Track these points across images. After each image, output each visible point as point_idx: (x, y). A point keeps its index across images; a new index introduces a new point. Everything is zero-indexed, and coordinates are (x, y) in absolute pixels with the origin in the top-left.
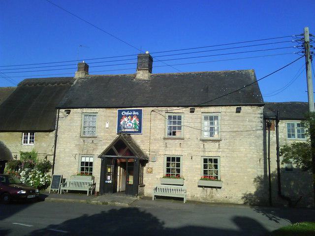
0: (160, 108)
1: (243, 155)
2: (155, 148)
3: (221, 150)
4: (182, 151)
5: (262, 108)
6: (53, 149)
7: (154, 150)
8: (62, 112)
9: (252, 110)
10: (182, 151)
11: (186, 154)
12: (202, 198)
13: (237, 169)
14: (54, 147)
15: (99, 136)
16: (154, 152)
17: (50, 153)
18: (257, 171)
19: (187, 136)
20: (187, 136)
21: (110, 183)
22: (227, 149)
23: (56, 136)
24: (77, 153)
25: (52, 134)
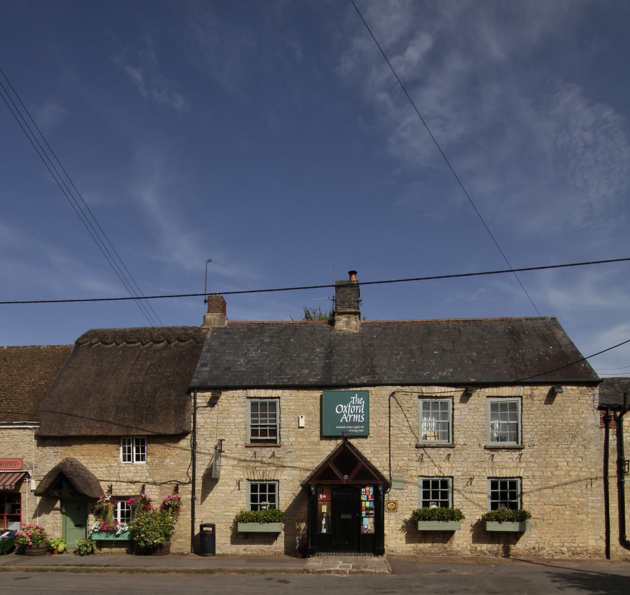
0: (407, 388)
1: (562, 473)
3: (523, 465)
4: (452, 468)
5: (597, 390)
6: (190, 471)
7: (399, 468)
8: (202, 398)
9: (578, 392)
10: (452, 468)
11: (460, 474)
12: (490, 552)
13: (552, 499)
14: (191, 467)
15: (285, 444)
16: (399, 472)
17: (183, 480)
18: (588, 500)
19: (460, 440)
20: (460, 440)
22: (535, 462)
23: (194, 445)
24: (242, 477)
25: (185, 443)
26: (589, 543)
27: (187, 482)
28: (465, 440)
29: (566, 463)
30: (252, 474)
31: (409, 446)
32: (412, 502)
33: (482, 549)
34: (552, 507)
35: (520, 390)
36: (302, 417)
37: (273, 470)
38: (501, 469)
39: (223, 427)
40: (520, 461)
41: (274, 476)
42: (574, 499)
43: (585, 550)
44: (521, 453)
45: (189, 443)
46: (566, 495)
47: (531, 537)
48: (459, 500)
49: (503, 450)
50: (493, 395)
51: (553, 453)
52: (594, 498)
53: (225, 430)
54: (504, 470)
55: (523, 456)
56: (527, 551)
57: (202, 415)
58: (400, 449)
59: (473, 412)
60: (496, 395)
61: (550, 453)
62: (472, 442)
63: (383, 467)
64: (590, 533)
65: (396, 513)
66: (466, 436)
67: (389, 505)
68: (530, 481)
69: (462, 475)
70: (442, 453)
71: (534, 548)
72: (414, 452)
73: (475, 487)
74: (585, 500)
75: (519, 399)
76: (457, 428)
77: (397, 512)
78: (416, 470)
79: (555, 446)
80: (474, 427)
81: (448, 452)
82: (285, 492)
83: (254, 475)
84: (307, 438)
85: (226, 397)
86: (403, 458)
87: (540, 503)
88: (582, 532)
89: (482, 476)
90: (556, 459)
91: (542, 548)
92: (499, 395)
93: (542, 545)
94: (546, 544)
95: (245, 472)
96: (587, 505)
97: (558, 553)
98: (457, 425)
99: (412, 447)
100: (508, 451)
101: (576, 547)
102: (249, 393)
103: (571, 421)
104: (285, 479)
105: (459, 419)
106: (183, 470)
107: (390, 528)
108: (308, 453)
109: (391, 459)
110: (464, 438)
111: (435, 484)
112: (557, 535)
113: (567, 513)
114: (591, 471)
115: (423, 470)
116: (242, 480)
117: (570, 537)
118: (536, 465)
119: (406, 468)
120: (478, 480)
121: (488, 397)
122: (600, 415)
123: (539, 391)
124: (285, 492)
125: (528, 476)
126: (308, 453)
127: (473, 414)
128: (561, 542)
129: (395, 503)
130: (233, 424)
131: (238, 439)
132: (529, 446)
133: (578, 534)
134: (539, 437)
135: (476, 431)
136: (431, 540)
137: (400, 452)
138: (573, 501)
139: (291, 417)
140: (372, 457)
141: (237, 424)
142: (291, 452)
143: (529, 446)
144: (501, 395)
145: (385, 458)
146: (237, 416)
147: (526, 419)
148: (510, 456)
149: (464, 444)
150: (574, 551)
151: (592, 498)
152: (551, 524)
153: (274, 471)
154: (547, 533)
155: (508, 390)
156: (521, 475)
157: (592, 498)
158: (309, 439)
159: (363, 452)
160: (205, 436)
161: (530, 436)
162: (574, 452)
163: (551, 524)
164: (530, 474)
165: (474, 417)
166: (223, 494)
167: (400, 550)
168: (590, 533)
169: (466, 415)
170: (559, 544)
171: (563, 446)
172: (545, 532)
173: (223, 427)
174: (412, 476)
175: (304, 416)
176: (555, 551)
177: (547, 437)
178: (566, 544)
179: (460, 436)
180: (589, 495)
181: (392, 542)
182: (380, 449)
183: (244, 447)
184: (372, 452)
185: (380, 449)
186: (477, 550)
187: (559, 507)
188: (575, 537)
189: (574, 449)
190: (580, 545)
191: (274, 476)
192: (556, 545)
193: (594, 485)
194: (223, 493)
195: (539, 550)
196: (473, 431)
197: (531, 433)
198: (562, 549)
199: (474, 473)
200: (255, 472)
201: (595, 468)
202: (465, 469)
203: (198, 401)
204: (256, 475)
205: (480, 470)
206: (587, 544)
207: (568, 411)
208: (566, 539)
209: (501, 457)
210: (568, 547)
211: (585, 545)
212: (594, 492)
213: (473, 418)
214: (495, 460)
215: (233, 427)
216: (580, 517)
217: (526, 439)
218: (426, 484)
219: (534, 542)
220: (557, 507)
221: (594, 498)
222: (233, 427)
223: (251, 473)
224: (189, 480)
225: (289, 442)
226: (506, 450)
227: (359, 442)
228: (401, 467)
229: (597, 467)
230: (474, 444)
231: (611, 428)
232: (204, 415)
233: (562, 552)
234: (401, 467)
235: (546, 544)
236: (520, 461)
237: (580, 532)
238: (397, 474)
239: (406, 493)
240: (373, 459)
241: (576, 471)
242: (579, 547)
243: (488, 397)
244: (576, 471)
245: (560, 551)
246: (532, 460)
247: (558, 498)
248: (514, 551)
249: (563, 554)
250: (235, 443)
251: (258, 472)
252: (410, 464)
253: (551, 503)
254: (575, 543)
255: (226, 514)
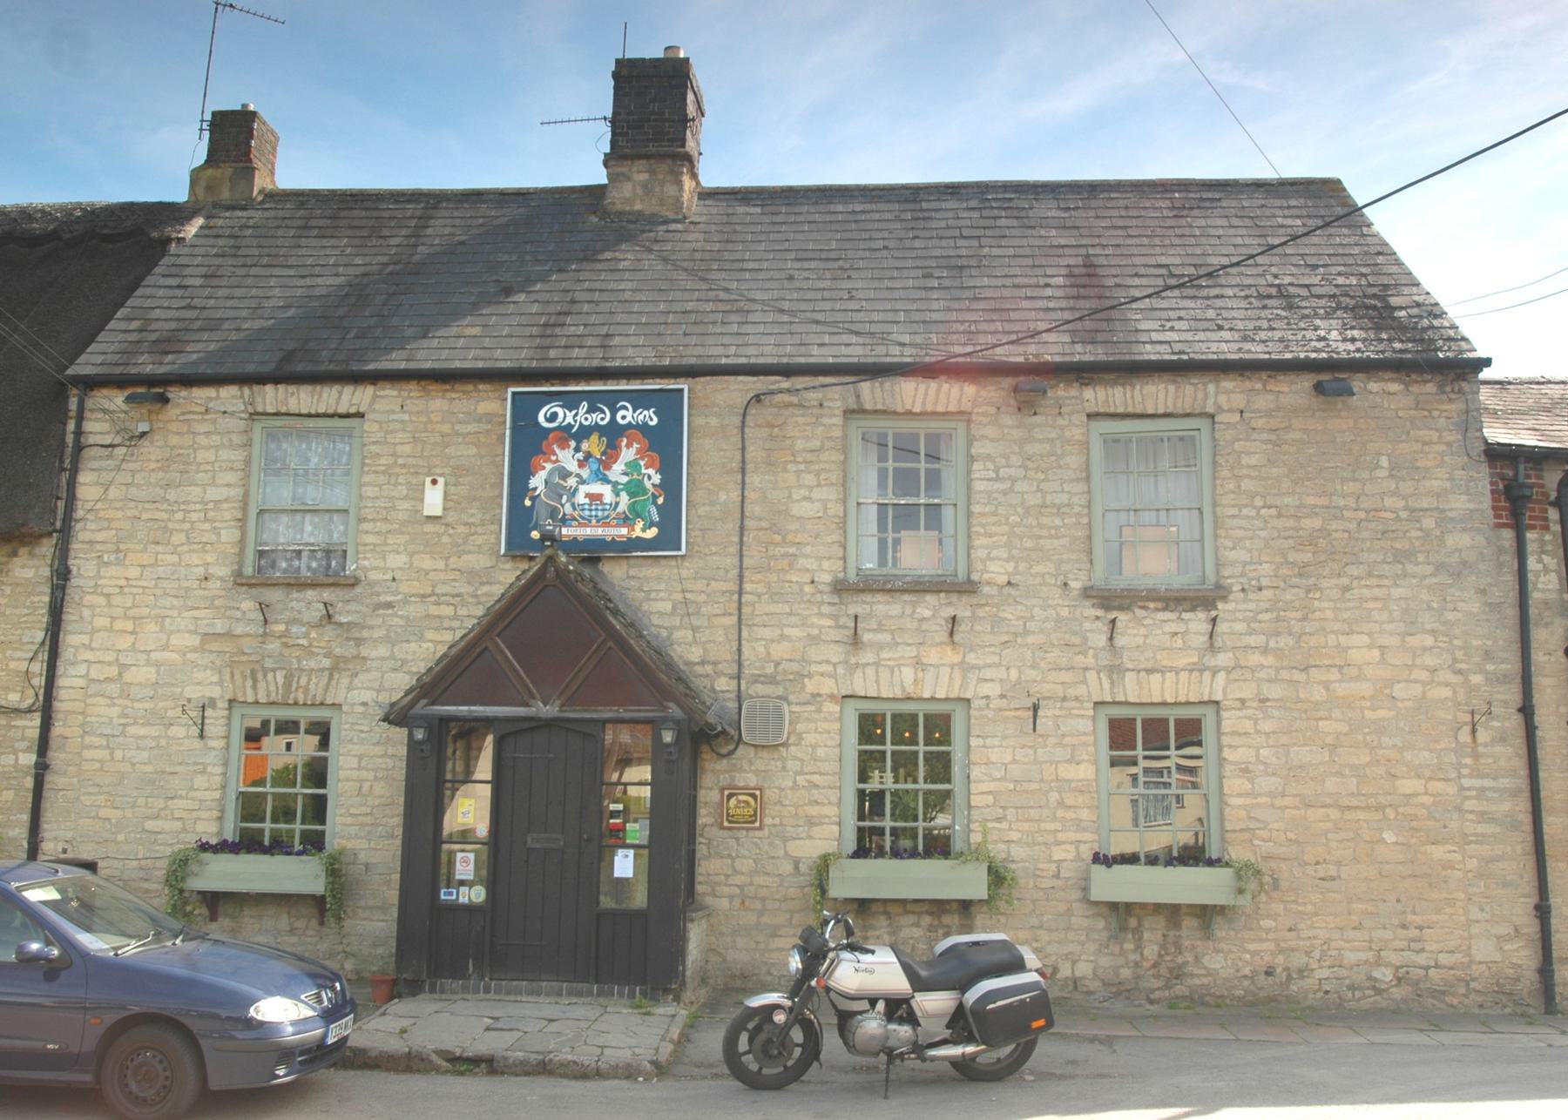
1: (1366, 688)
2: (778, 651)
3: (1223, 659)
4: (966, 668)
6: (39, 667)
7: (770, 669)
9: (1410, 400)
10: (966, 668)
11: (993, 690)
12: (1105, 984)
13: (1331, 784)
15: (373, 576)
16: (771, 680)
18: (1462, 788)
19: (992, 566)
20: (992, 566)
21: (470, 909)
22: (1265, 650)
23: (62, 576)
24: (215, 692)
26: (1473, 952)
27: (25, 705)
28: (1010, 567)
29: (1376, 653)
30: (249, 683)
31: (807, 589)
32: (815, 792)
33: (1078, 974)
34: (1334, 814)
35: (1206, 396)
36: (434, 482)
37: (322, 670)
38: (1143, 674)
39: (164, 516)
40: (1212, 645)
41: (326, 689)
42: (1408, 785)
43: (1459, 979)
44: (1214, 613)
45: (46, 572)
46: (1382, 770)
47: (1261, 928)
48: (992, 786)
49: (1152, 605)
50: (1112, 410)
51: (1329, 614)
52: (1487, 783)
53: (170, 525)
54: (1155, 678)
55: (1222, 627)
56: (1246, 983)
57: (96, 474)
58: (776, 598)
59: (1037, 470)
60: (1121, 410)
61: (1318, 615)
62: (1035, 576)
63: (715, 664)
64: (1475, 914)
65: (758, 833)
66: (1014, 552)
67: (733, 802)
68: (1249, 718)
69: (1002, 696)
70: (927, 613)
71: (1269, 973)
72: (826, 609)
73: (1052, 741)
74: (1451, 789)
75: (1203, 424)
76: (983, 526)
77: (760, 828)
78: (834, 676)
79: (1336, 594)
80: (1045, 520)
81: (950, 612)
82: (357, 749)
83: (254, 687)
84: (447, 559)
85: (183, 414)
86: (787, 631)
87: (1288, 801)
88: (1447, 910)
89: (1077, 699)
90: (1342, 639)
91: (1300, 972)
92: (1130, 410)
93: (1298, 960)
94: (1317, 954)
95: (227, 677)
96: (1459, 809)
97: (1359, 988)
98: (983, 514)
99: (821, 592)
100: (1165, 609)
101: (1427, 968)
102: (259, 400)
103: (1389, 502)
104: (364, 704)
105: (989, 493)
106: (12, 665)
107: (737, 891)
108: (449, 611)
109: (745, 634)
110: (1007, 560)
111: (904, 723)
112: (1355, 918)
113: (1389, 837)
114: (1467, 681)
115: (858, 674)
116: (212, 703)
117: (1404, 926)
118: (1269, 660)
119: (795, 667)
120: (1058, 712)
121: (1091, 416)
122: (1492, 483)
123: (1271, 397)
124: (357, 749)
125: (1243, 701)
126: (449, 611)
127: (1041, 476)
128: (1371, 949)
129: (754, 796)
130: (198, 507)
131: (210, 558)
132: (1243, 590)
133: (1434, 918)
134: (1278, 559)
135: (1051, 537)
136: (886, 938)
137: (778, 608)
138: (1408, 791)
139: (396, 484)
140: (675, 628)
141: (211, 505)
142: (389, 605)
143: (1243, 590)
144: (1139, 410)
145: (721, 632)
146: (214, 478)
147: (1232, 496)
148: (1173, 627)
149: (1009, 583)
150: (1417, 983)
151: (1477, 783)
152: (1333, 879)
153: (326, 674)
154: (1316, 915)
155: (1161, 395)
156: (1218, 697)
157: (1477, 783)
158: (453, 559)
159: (645, 606)
160: (98, 547)
161: (1245, 556)
162: (1406, 611)
163: (1333, 879)
164: (1247, 692)
165: (1044, 486)
166: (145, 754)
167: (769, 973)
168: (1475, 914)
169: (1014, 480)
170: (1362, 956)
171: (1366, 593)
172: (1310, 908)
173: (164, 516)
174: (819, 695)
175: (441, 481)
176: (1347, 982)
177: (1307, 557)
178: (1391, 957)
179: (995, 553)
180: (1465, 771)
181: (740, 942)
182: (703, 597)
183: (230, 585)
184: (674, 608)
185: (703, 597)
186: (1059, 976)
187: (1361, 815)
188: (1421, 928)
189: (1402, 603)
190: (1444, 959)
191: (326, 689)
192: (1351, 957)
193: (1482, 736)
194: (144, 749)
195: (1289, 978)
196: (1040, 537)
197: (1248, 543)
198: (1376, 974)
199: (1046, 689)
200: (260, 676)
201: (1481, 671)
202: (1014, 674)
203: (88, 426)
204: (261, 685)
205: (1066, 677)
206: (1469, 955)
207: (1378, 467)
208: (1388, 934)
209: (1143, 631)
210: (1397, 968)
211: (1459, 957)
212: (1483, 761)
213: (1039, 490)
214: (1120, 641)
215: (194, 516)
216: (1438, 852)
217: (1232, 564)
218: (869, 727)
219: (1272, 946)
220: (1348, 815)
221: (1487, 783)
222: (194, 516)
223: (244, 678)
224: (30, 701)
225: (385, 569)
226: (1160, 605)
227: (632, 572)
228: (777, 664)
229: (1490, 667)
230: (1044, 584)
231: (1533, 527)
232: (104, 474)
233: (1374, 988)
234: (777, 664)
235: (1317, 954)
236: (1212, 645)
237: (1438, 911)
238: (759, 689)
239: (796, 758)
240: (678, 635)
241: (1416, 681)
242: (1437, 966)
243: (1091, 416)
244: (1416, 681)
245: (1368, 984)
246: (1252, 640)
247: (1354, 781)
248: (1197, 981)
249: (1379, 992)
250: (200, 571)
251: (270, 676)
252: (813, 653)
253: (1328, 801)
254: (1423, 950)
255: (149, 825)
